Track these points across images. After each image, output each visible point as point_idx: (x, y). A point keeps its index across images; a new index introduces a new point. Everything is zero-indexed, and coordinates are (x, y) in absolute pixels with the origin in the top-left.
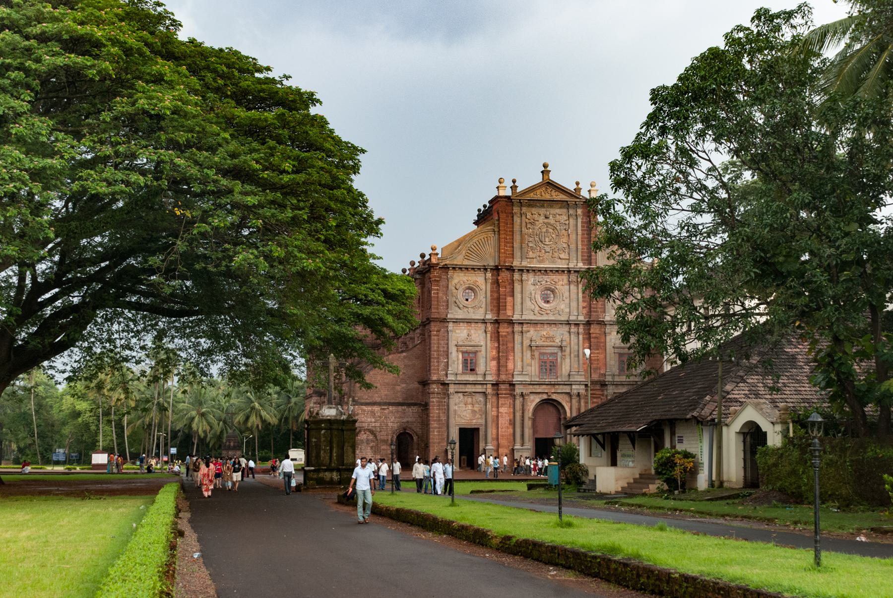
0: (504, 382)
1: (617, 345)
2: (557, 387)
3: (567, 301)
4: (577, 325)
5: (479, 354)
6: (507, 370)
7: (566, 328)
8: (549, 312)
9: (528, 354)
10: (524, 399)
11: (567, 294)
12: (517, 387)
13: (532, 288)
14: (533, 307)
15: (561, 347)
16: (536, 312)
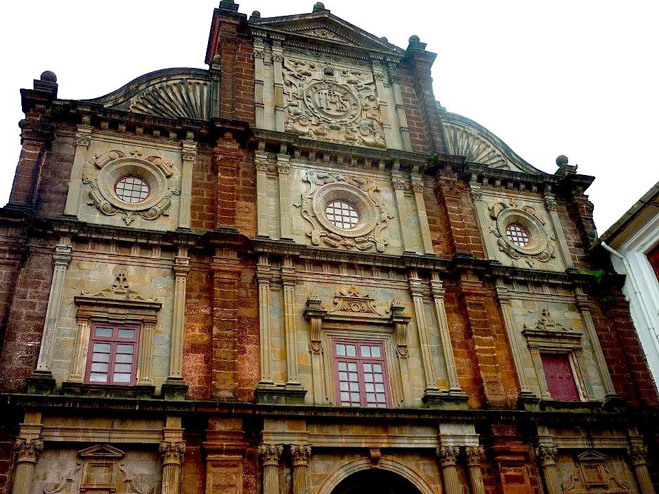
0: (226, 410)
1: (532, 327)
2: (395, 431)
3: (393, 224)
4: (425, 275)
5: (147, 331)
6: (235, 377)
7: (401, 282)
8: (348, 242)
9: (300, 341)
10: (291, 473)
11: (389, 210)
12: (268, 427)
13: (304, 187)
14: (307, 228)
15: (393, 323)
16: (316, 238)
